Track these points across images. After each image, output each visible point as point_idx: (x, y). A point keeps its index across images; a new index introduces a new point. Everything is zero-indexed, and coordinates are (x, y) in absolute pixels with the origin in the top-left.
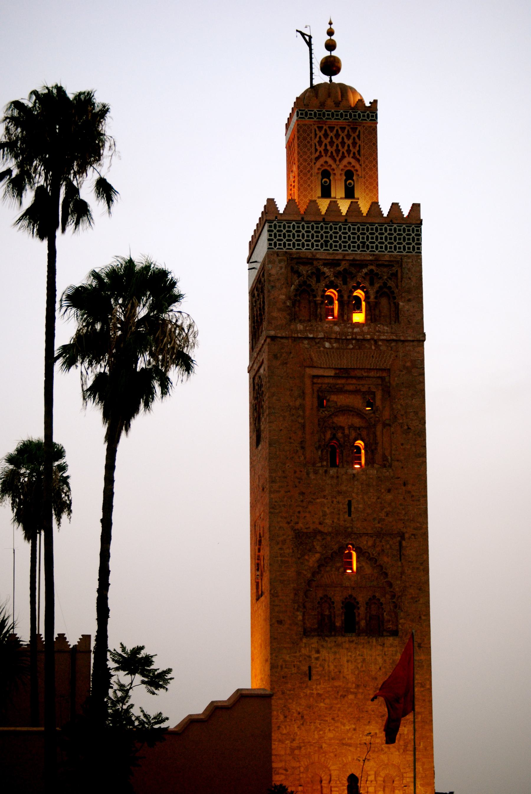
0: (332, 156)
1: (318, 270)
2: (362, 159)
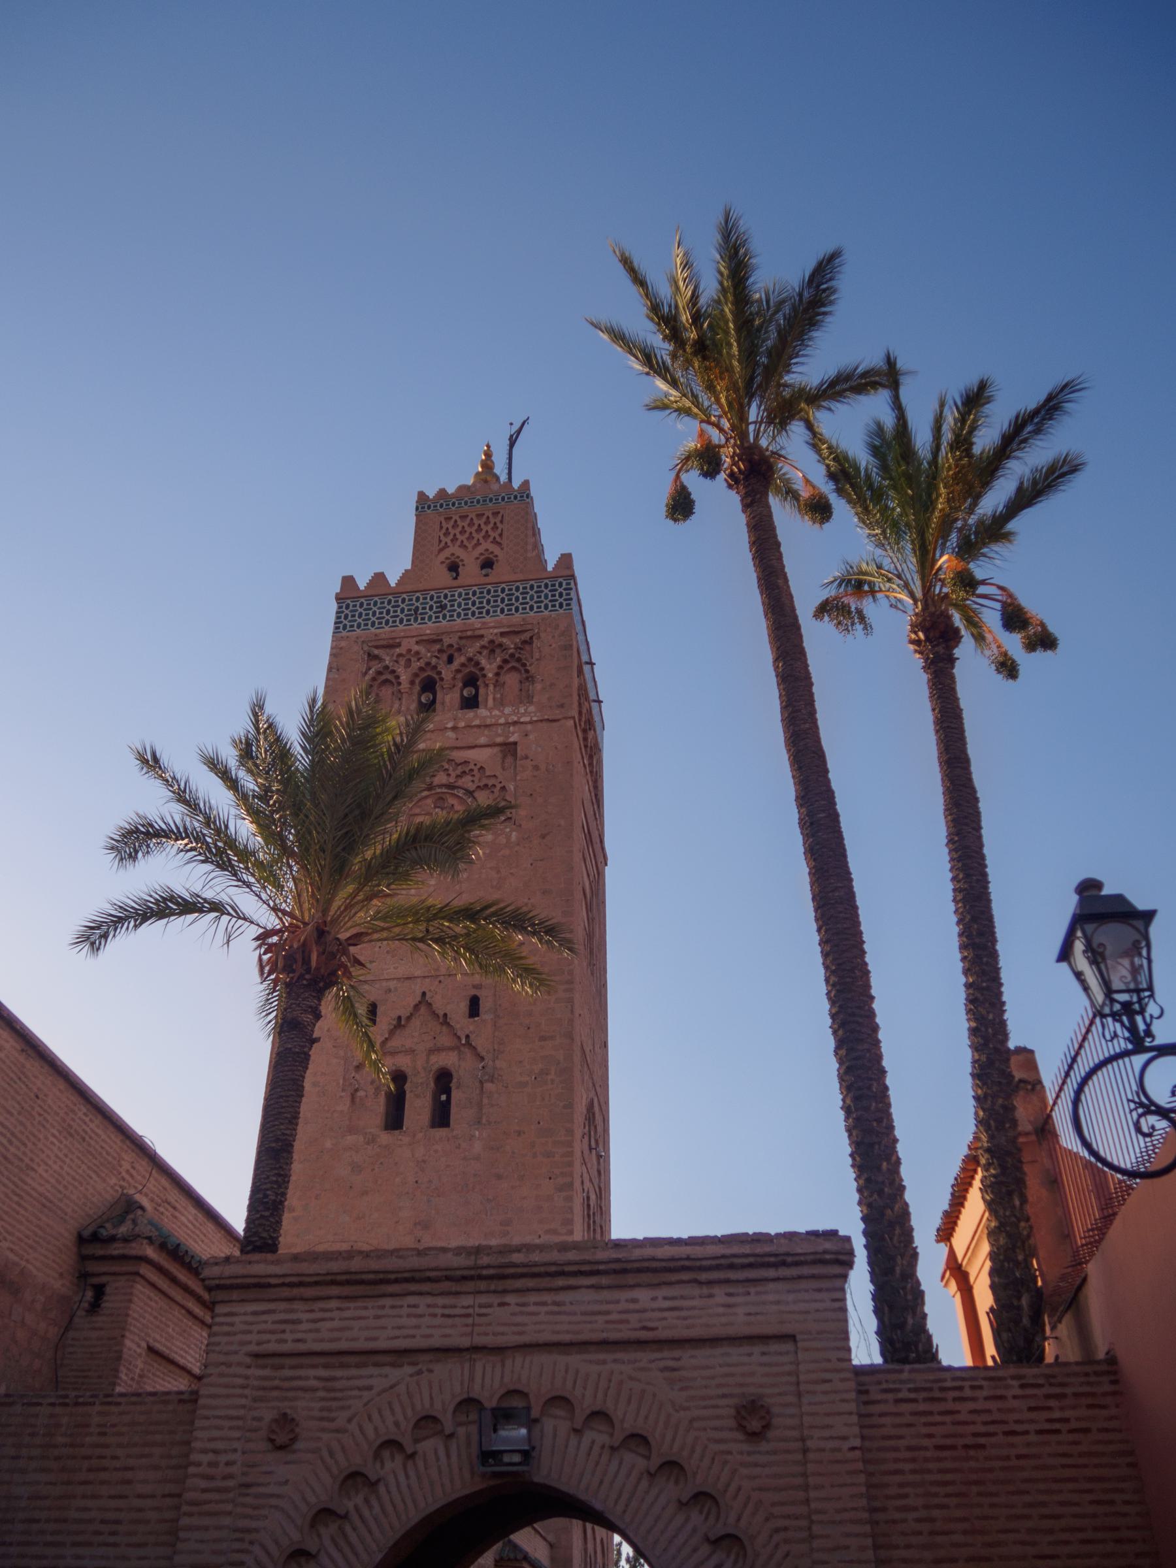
0: (462, 546)
1: (409, 651)
2: (504, 542)
